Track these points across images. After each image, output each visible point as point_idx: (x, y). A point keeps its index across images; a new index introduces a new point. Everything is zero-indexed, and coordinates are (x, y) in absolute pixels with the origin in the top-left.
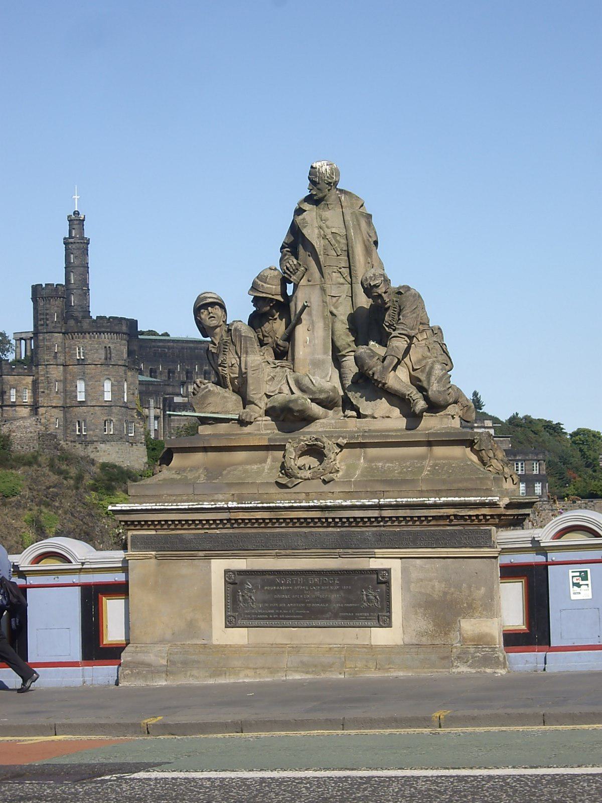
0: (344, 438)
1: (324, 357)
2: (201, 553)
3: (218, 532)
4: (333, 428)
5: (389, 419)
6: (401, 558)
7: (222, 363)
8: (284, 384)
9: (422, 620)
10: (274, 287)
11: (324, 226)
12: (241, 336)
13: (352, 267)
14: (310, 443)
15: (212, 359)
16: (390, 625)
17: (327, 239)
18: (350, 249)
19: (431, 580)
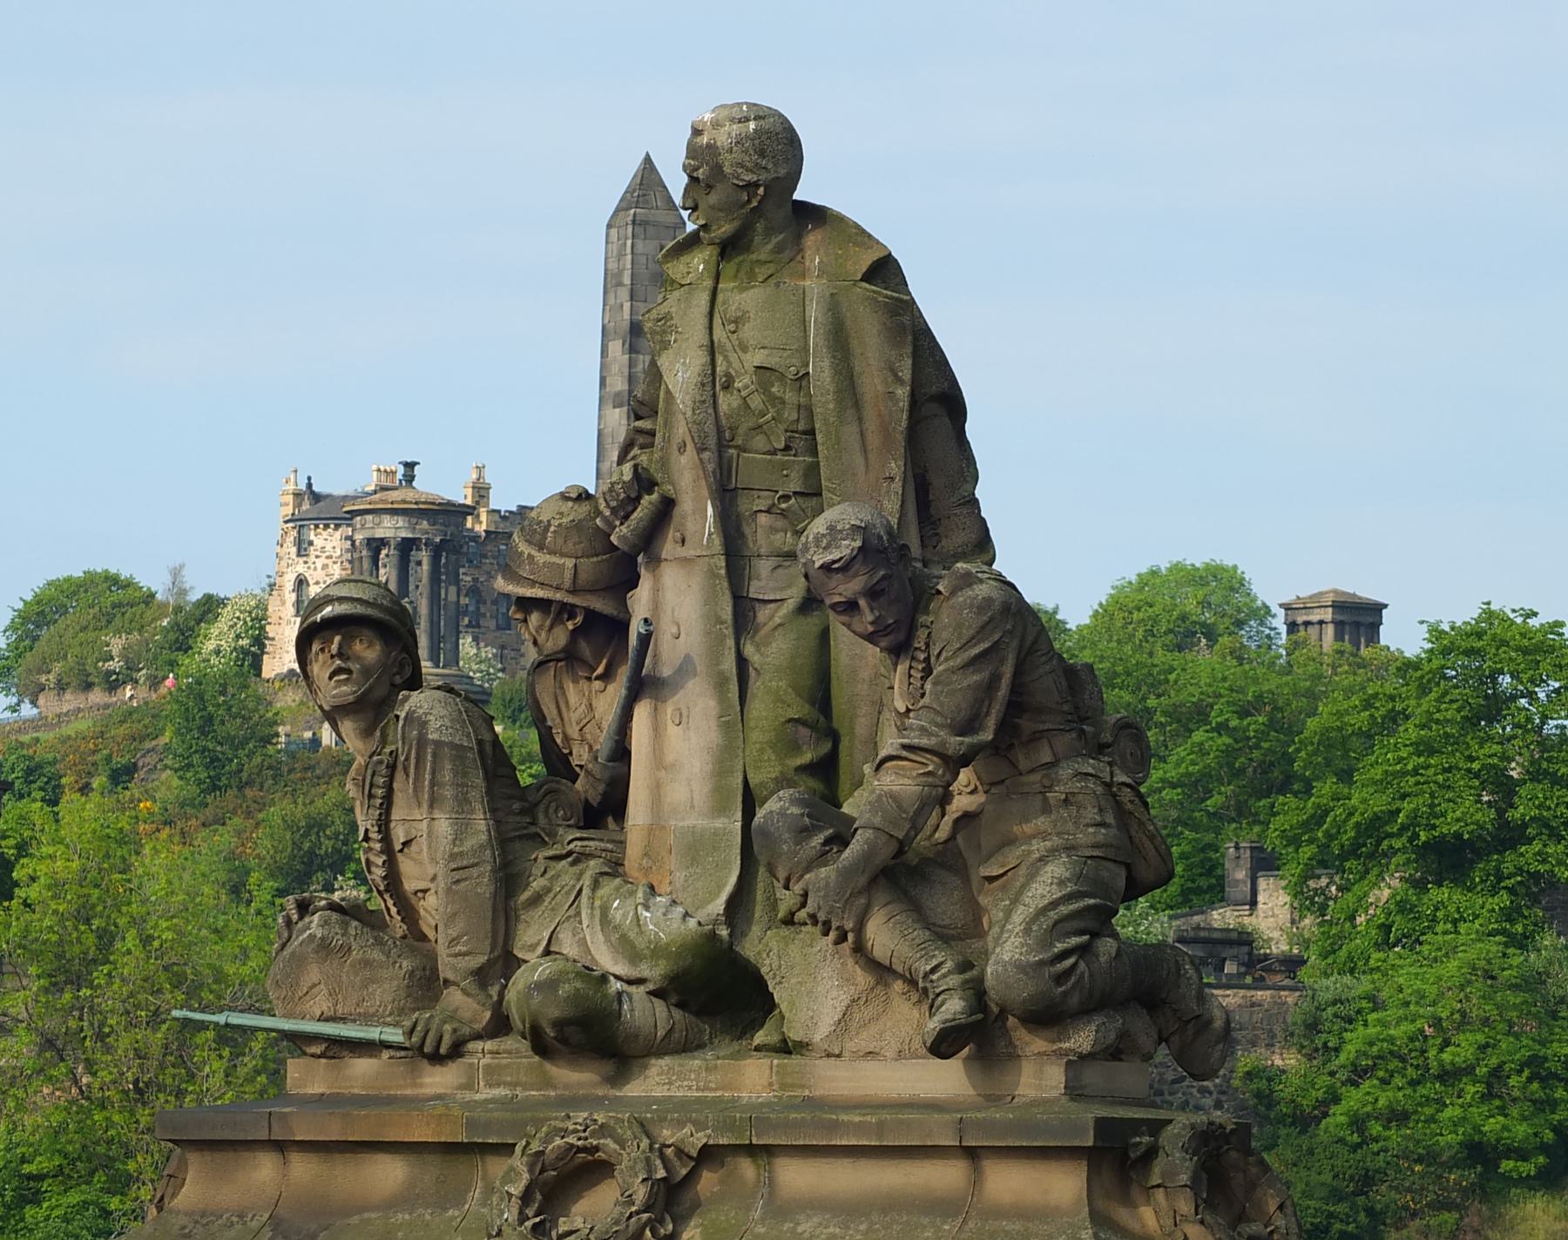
0: (700, 1126)
1: (719, 823)
4: (698, 1089)
10: (570, 563)
12: (422, 742)
14: (580, 1143)
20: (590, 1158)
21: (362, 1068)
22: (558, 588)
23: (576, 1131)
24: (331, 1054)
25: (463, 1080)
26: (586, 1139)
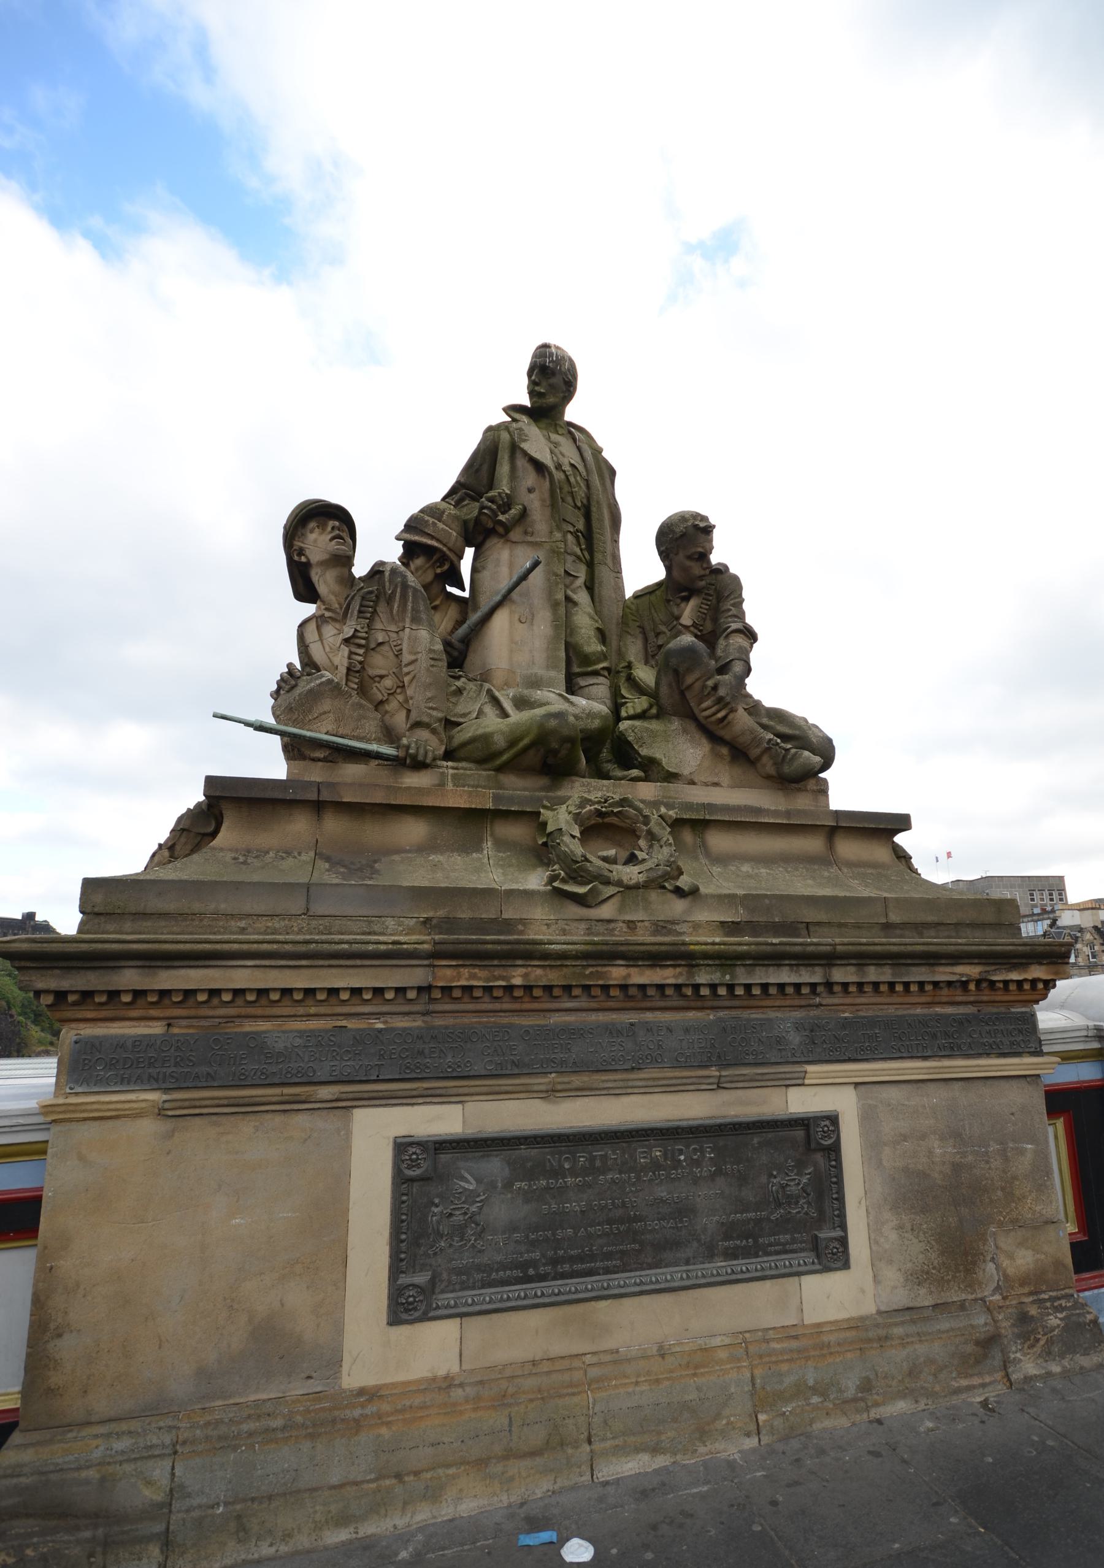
2: (325, 1092)
3: (380, 1026)
5: (717, 789)
6: (857, 1084)
7: (354, 636)
8: (486, 703)
9: (915, 1241)
11: (556, 450)
13: (596, 536)
14: (604, 809)
15: (317, 637)
16: (846, 1265)
17: (564, 472)
18: (593, 503)
19: (923, 1137)
20: (601, 821)
21: (352, 771)
22: (445, 545)
23: (599, 802)
24: (331, 759)
25: (436, 782)
26: (606, 807)
